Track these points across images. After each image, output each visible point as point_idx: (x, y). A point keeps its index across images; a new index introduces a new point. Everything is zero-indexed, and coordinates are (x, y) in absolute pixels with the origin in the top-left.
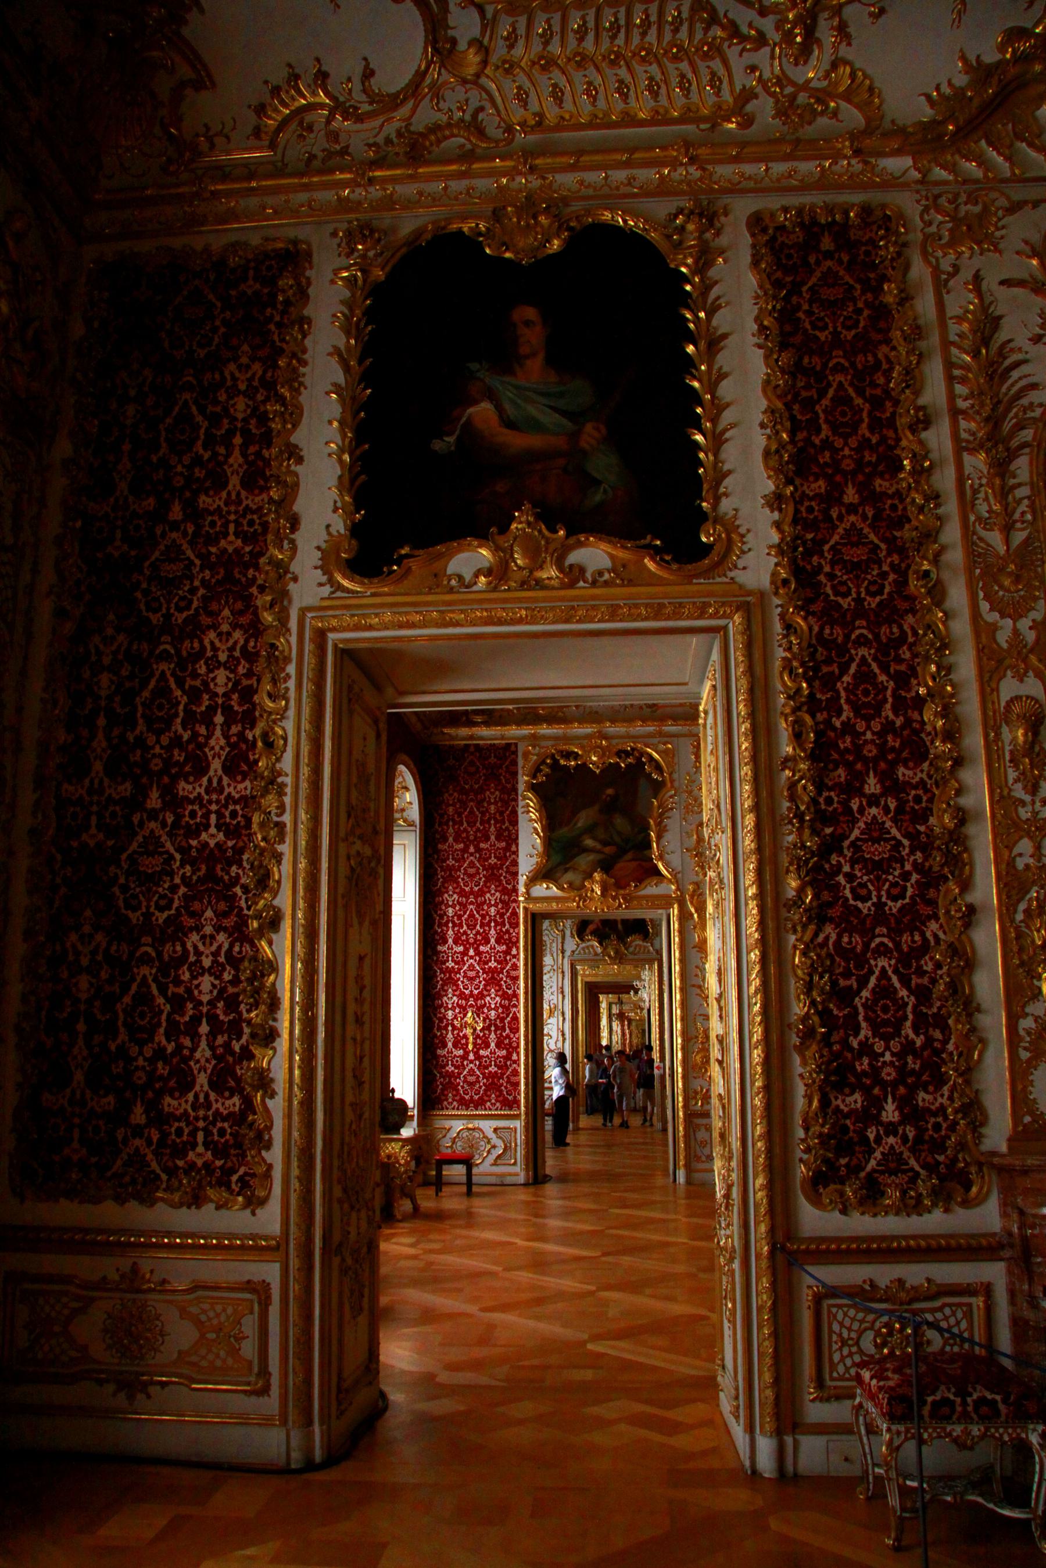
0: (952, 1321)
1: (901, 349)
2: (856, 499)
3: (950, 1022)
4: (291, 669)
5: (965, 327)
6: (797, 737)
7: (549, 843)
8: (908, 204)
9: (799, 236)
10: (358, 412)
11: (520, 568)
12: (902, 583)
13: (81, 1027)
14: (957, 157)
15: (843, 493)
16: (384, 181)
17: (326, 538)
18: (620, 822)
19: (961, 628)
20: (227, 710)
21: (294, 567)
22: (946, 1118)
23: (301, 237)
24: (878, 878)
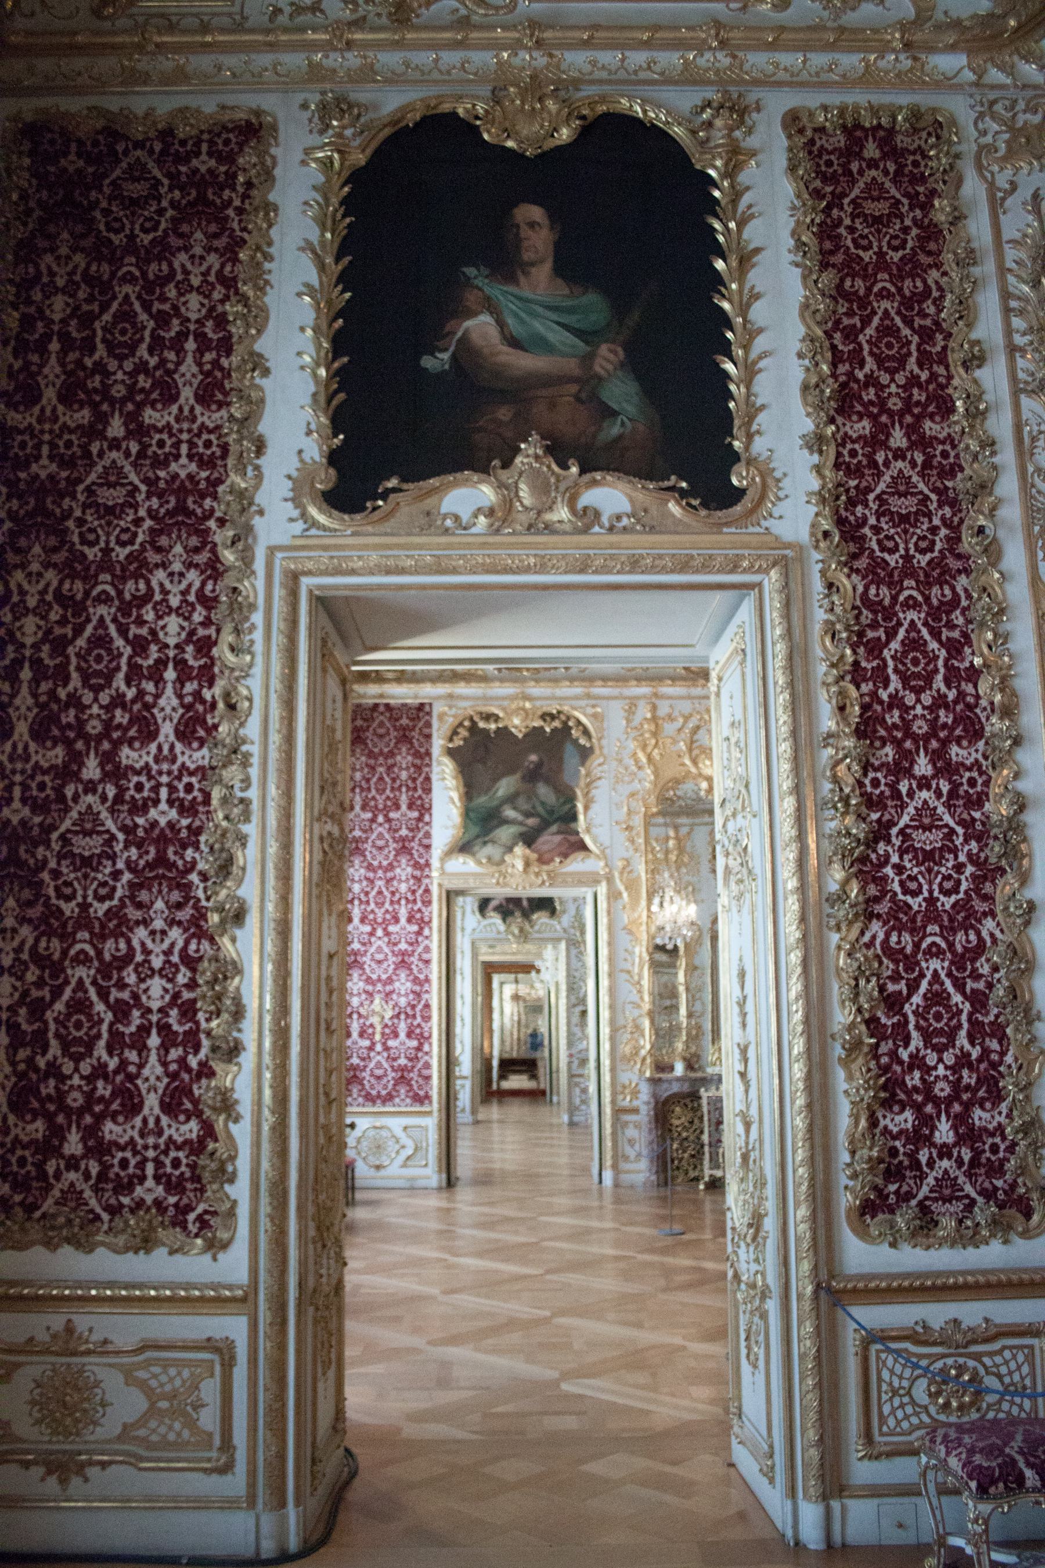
0: (1013, 1365)
1: (953, 274)
2: (904, 443)
3: (1008, 1031)
4: (257, 618)
5: (1023, 255)
6: (842, 709)
7: (467, 813)
8: (960, 108)
9: (840, 140)
10: (335, 319)
11: (526, 508)
12: (954, 540)
14: (1016, 58)
15: (888, 435)
16: (366, 45)
17: (299, 465)
18: (543, 791)
20: (181, 664)
21: (260, 498)
22: (1004, 1138)
23: (265, 107)
24: (929, 870)
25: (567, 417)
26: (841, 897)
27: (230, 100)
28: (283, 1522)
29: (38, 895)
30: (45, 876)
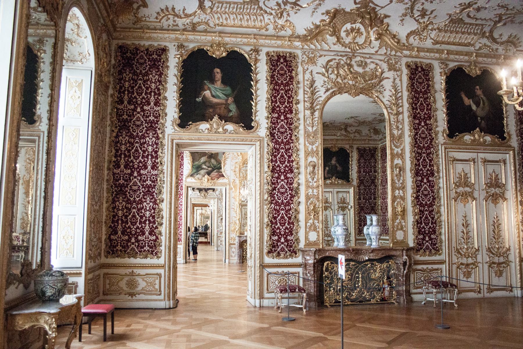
4: (166, 147)
5: (308, 83)
6: (269, 167)
8: (299, 53)
9: (276, 58)
13: (120, 222)
18: (213, 161)
19: (301, 147)
25: (222, 111)
26: (267, 200)
27: (160, 43)
28: (170, 303)
29: (126, 197)
30: (127, 193)
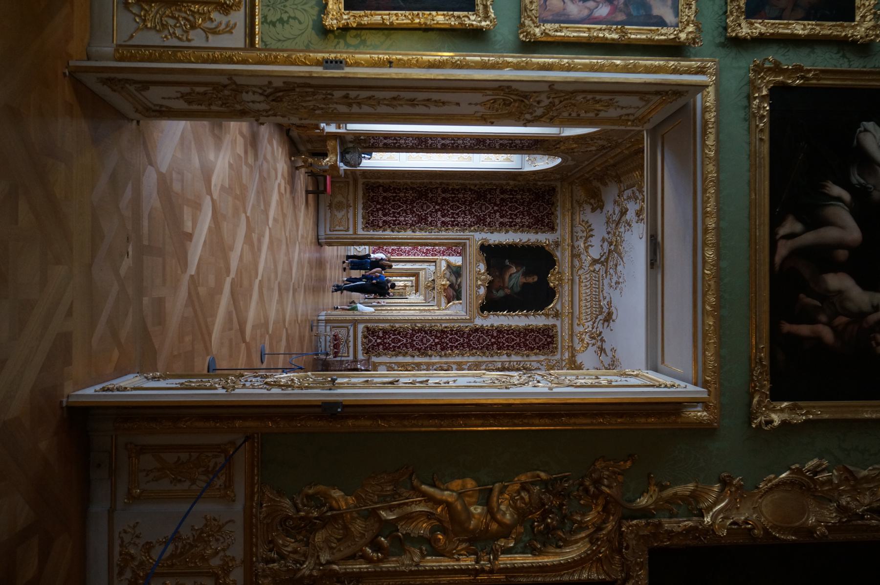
8: (558, 357)
19: (465, 359)
